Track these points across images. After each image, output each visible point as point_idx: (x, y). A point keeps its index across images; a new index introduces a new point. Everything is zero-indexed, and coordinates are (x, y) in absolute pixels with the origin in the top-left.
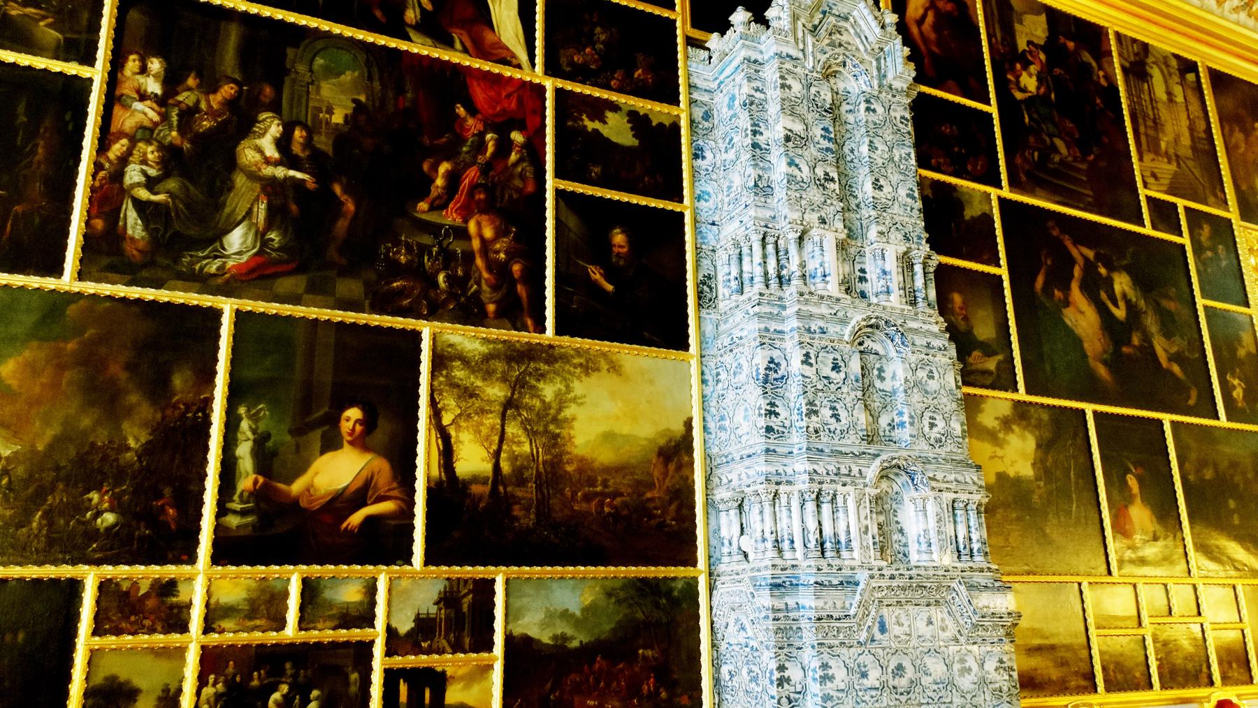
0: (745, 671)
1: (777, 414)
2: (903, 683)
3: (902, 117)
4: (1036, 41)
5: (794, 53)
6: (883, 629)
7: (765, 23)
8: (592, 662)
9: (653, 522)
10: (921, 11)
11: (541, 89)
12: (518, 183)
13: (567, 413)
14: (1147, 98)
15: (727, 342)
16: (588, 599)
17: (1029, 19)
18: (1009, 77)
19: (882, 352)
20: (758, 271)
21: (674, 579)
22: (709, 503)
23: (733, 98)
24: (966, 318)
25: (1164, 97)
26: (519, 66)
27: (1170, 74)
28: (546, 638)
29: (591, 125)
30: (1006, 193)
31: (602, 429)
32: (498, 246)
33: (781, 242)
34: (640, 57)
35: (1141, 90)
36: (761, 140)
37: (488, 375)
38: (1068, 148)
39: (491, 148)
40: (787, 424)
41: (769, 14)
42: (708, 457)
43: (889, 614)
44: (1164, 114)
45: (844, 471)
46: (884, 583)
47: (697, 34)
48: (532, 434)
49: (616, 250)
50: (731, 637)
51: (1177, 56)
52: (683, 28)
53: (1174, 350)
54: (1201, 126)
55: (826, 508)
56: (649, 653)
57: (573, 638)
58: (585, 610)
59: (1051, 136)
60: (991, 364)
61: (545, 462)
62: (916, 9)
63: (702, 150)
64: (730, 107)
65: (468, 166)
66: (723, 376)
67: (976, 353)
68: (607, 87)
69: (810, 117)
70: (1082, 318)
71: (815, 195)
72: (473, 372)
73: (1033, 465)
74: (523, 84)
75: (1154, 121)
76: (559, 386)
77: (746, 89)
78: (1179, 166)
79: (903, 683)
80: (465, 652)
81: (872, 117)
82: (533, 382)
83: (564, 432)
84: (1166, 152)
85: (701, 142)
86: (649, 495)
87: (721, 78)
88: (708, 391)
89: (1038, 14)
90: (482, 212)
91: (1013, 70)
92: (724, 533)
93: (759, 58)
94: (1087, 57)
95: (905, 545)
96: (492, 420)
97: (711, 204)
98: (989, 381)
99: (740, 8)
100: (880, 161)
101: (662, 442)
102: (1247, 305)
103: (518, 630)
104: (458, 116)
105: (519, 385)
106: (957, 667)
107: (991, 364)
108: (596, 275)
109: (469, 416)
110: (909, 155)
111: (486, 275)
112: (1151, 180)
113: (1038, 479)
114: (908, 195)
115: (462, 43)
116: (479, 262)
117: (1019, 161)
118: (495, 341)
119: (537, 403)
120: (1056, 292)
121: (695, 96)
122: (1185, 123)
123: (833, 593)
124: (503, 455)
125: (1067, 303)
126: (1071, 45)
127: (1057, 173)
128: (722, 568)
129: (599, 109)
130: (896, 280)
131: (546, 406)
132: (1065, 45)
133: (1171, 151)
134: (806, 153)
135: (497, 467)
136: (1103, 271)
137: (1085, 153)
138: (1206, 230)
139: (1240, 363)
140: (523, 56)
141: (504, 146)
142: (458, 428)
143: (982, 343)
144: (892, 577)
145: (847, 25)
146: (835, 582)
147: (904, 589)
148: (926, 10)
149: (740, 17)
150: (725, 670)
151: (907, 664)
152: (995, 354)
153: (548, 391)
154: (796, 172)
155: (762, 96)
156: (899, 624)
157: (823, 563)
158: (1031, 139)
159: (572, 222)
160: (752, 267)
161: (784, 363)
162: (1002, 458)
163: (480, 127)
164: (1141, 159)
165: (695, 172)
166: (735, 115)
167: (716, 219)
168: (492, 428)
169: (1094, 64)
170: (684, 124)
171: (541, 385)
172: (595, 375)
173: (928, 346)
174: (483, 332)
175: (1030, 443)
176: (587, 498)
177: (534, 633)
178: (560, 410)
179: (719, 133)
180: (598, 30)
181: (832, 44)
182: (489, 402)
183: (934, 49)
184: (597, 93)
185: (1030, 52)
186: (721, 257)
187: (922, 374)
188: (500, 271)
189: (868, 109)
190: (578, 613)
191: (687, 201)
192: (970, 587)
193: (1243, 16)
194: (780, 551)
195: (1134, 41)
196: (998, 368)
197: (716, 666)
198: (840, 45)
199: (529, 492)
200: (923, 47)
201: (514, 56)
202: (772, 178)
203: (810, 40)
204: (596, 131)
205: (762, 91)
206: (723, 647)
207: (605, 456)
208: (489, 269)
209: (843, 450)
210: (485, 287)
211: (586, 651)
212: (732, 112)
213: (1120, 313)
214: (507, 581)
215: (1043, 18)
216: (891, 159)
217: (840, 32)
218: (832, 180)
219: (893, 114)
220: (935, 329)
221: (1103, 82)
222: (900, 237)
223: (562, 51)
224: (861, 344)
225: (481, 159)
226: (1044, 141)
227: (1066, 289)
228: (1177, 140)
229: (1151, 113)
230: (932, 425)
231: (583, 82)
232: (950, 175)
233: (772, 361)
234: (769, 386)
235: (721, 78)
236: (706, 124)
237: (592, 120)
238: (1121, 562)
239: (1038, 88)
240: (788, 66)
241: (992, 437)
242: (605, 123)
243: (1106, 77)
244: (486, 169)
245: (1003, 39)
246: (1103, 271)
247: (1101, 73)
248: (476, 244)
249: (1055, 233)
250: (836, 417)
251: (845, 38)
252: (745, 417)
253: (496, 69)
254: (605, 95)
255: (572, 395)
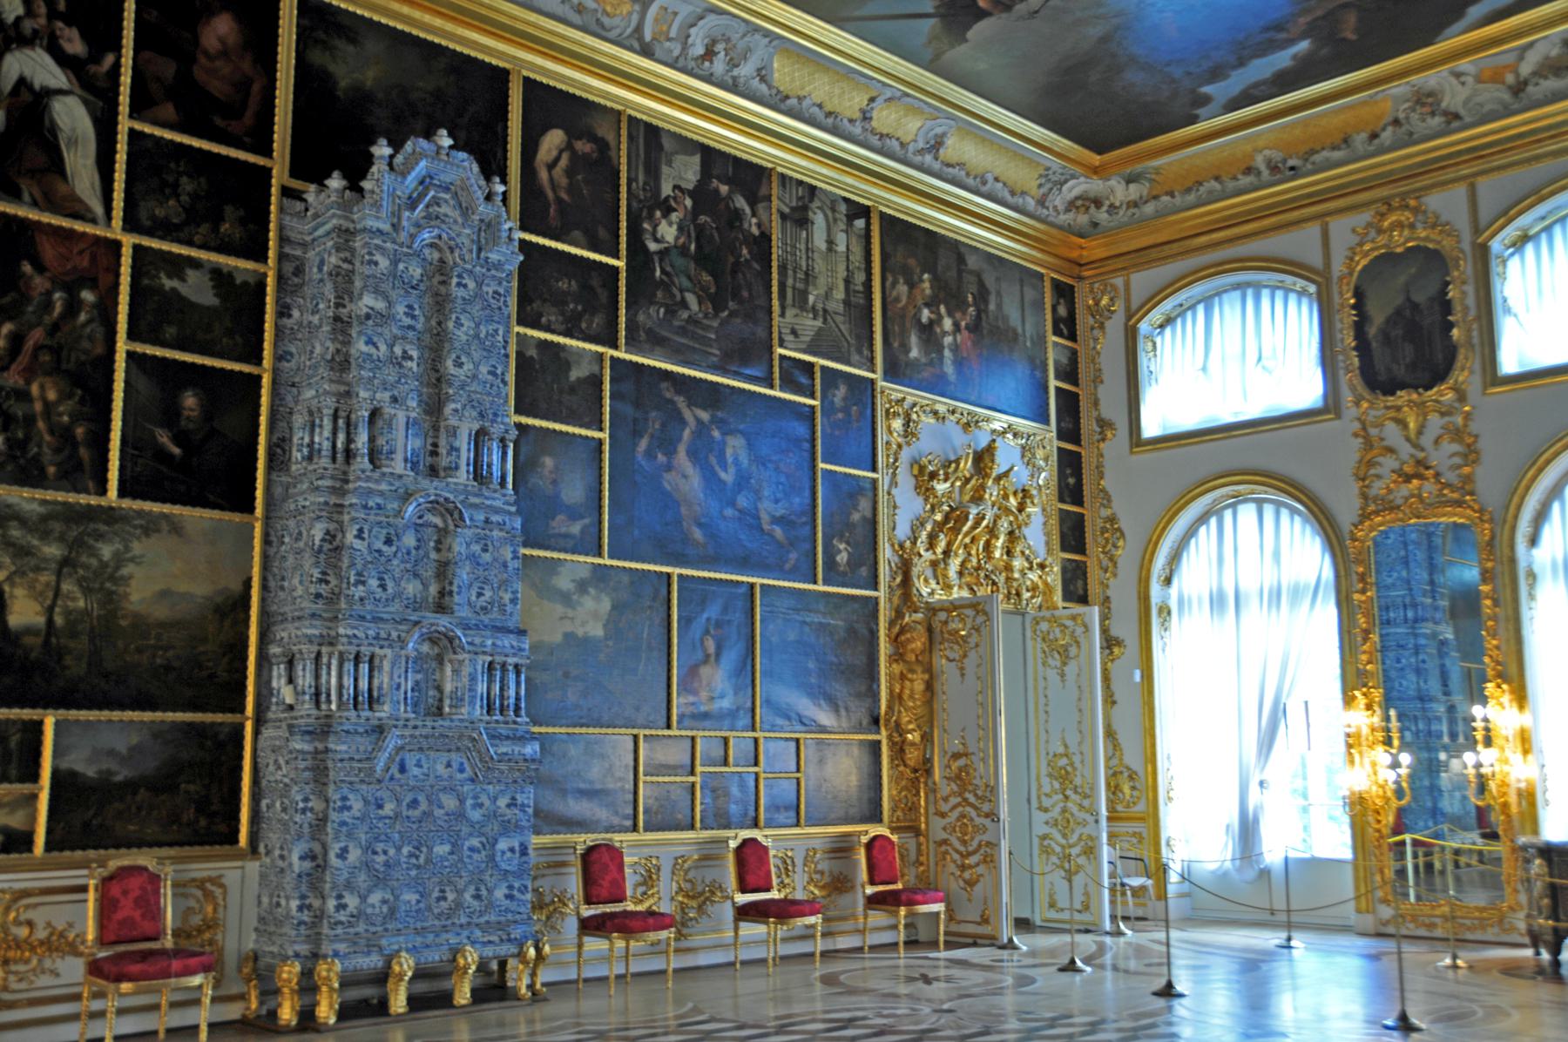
0: (278, 804)
1: (327, 582)
2: (416, 813)
3: (495, 292)
4: (684, 185)
5: (386, 227)
6: (403, 769)
7: (360, 191)
8: (135, 794)
9: (205, 673)
10: (555, 153)
11: (117, 245)
12: (85, 344)
13: (125, 571)
14: (803, 247)
15: (292, 507)
16: (135, 740)
17: (679, 159)
18: (646, 226)
19: (440, 523)
20: (326, 445)
21: (221, 724)
22: (264, 659)
23: (322, 263)
24: (554, 482)
25: (824, 246)
26: (94, 221)
27: (835, 220)
28: (91, 772)
29: (169, 284)
30: (621, 354)
31: (158, 588)
32: (61, 409)
33: (353, 416)
34: (229, 210)
35: (797, 239)
36: (343, 312)
37: (45, 535)
38: (700, 303)
39: (58, 308)
40: (337, 590)
41: (366, 185)
42: (264, 613)
43: (411, 759)
44: (819, 265)
45: (383, 635)
46: (407, 732)
47: (296, 184)
48: (87, 591)
49: (186, 413)
50: (271, 775)
51: (846, 200)
52: (280, 174)
53: (780, 512)
54: (860, 278)
55: (364, 668)
56: (192, 788)
57: (116, 773)
58: (132, 749)
59: (681, 291)
60: (576, 529)
61: (99, 617)
62: (550, 150)
63: (288, 307)
64: (320, 270)
65: (32, 327)
66: (287, 540)
67: (560, 517)
68: (190, 243)
69: (393, 295)
70: (686, 479)
71: (390, 374)
72: (30, 531)
73: (605, 626)
74: (98, 240)
75: (807, 274)
76: (118, 546)
77: (333, 260)
78: (825, 320)
79: (416, 813)
80: (10, 782)
81: (461, 292)
82: (91, 542)
83: (121, 590)
84: (813, 307)
85: (288, 300)
86: (201, 649)
87: (317, 234)
88: (272, 551)
89: (692, 154)
90: (48, 374)
91: (651, 216)
92: (274, 684)
93: (351, 226)
94: (741, 202)
95: (441, 700)
96: (46, 578)
97: (293, 365)
98: (571, 543)
99: (336, 174)
100: (464, 338)
101: (219, 600)
102: (874, 470)
103: (64, 765)
104: (24, 274)
105: (78, 544)
106: (469, 802)
107: (576, 529)
108: (164, 438)
109: (24, 574)
110: (496, 331)
111: (47, 438)
112: (791, 338)
113: (606, 638)
114: (490, 373)
115: (31, 195)
116: (41, 424)
117: (641, 318)
118: (55, 503)
119: (94, 562)
120: (660, 456)
121: (287, 250)
122: (842, 273)
123: (358, 739)
124: (57, 610)
125: (669, 468)
126: (724, 189)
127: (683, 331)
128: (270, 715)
129: (178, 266)
130: (466, 453)
131: (104, 565)
132: (717, 191)
133: (820, 306)
134: (386, 331)
135: (50, 622)
136: (716, 434)
137: (718, 309)
138: (841, 392)
139: (850, 526)
140: (99, 209)
141: (73, 306)
142: (13, 585)
143: (568, 507)
144: (415, 727)
145: (447, 196)
146: (361, 730)
147: (426, 737)
148: (561, 152)
149: (335, 182)
150: (264, 803)
151: (422, 798)
152: (582, 517)
153: (106, 551)
154: (373, 350)
155: (350, 267)
156: (419, 765)
157: (353, 713)
158: (659, 294)
159: (142, 383)
160: (322, 438)
161: (339, 536)
162: (572, 619)
163: (48, 285)
164: (783, 315)
165: (279, 332)
166: (321, 280)
167: (297, 380)
168: (47, 584)
169: (748, 210)
170: (270, 281)
171: (99, 545)
172: (154, 538)
173: (487, 521)
174: (39, 494)
175: (606, 605)
176: (139, 651)
177: (80, 767)
178: (118, 568)
179: (308, 291)
180: (184, 179)
181: (428, 217)
182: (46, 560)
183: (564, 196)
184: (176, 249)
185: (675, 198)
186: (299, 420)
187: (476, 548)
188: (65, 437)
189: (459, 284)
190: (124, 751)
191: (267, 362)
192: (492, 737)
193: (928, 159)
194: (318, 704)
195: (800, 183)
196: (583, 531)
197: (256, 798)
198: (437, 217)
199: (82, 644)
200: (550, 194)
201: (89, 209)
202: (353, 351)
203: (407, 214)
204: (173, 290)
205: (350, 262)
206: (264, 783)
207: (161, 612)
208: (51, 432)
209: (385, 616)
210: (46, 449)
211: (130, 786)
212: (319, 276)
213: (728, 477)
214: (57, 724)
215: (697, 159)
216: (477, 336)
217: (438, 205)
218: (411, 358)
219: (485, 289)
220: (498, 504)
221: (755, 231)
222: (475, 414)
223: (142, 204)
224: (420, 517)
225: (47, 319)
226: (674, 296)
227: (671, 452)
228: (827, 295)
229: (804, 264)
230: (480, 595)
231: (162, 238)
232: (559, 334)
233: (328, 532)
234: (322, 556)
235: (317, 234)
236: (296, 280)
237: (170, 277)
238: (681, 717)
239: (677, 238)
240: (377, 241)
241: (566, 598)
242: (183, 280)
243: (759, 225)
244: (55, 328)
245: (645, 183)
246: (716, 434)
247: (754, 220)
248: (38, 407)
249: (668, 395)
250: (383, 587)
251: (444, 209)
252: (301, 582)
253: (66, 223)
254: (184, 251)
255: (129, 555)
